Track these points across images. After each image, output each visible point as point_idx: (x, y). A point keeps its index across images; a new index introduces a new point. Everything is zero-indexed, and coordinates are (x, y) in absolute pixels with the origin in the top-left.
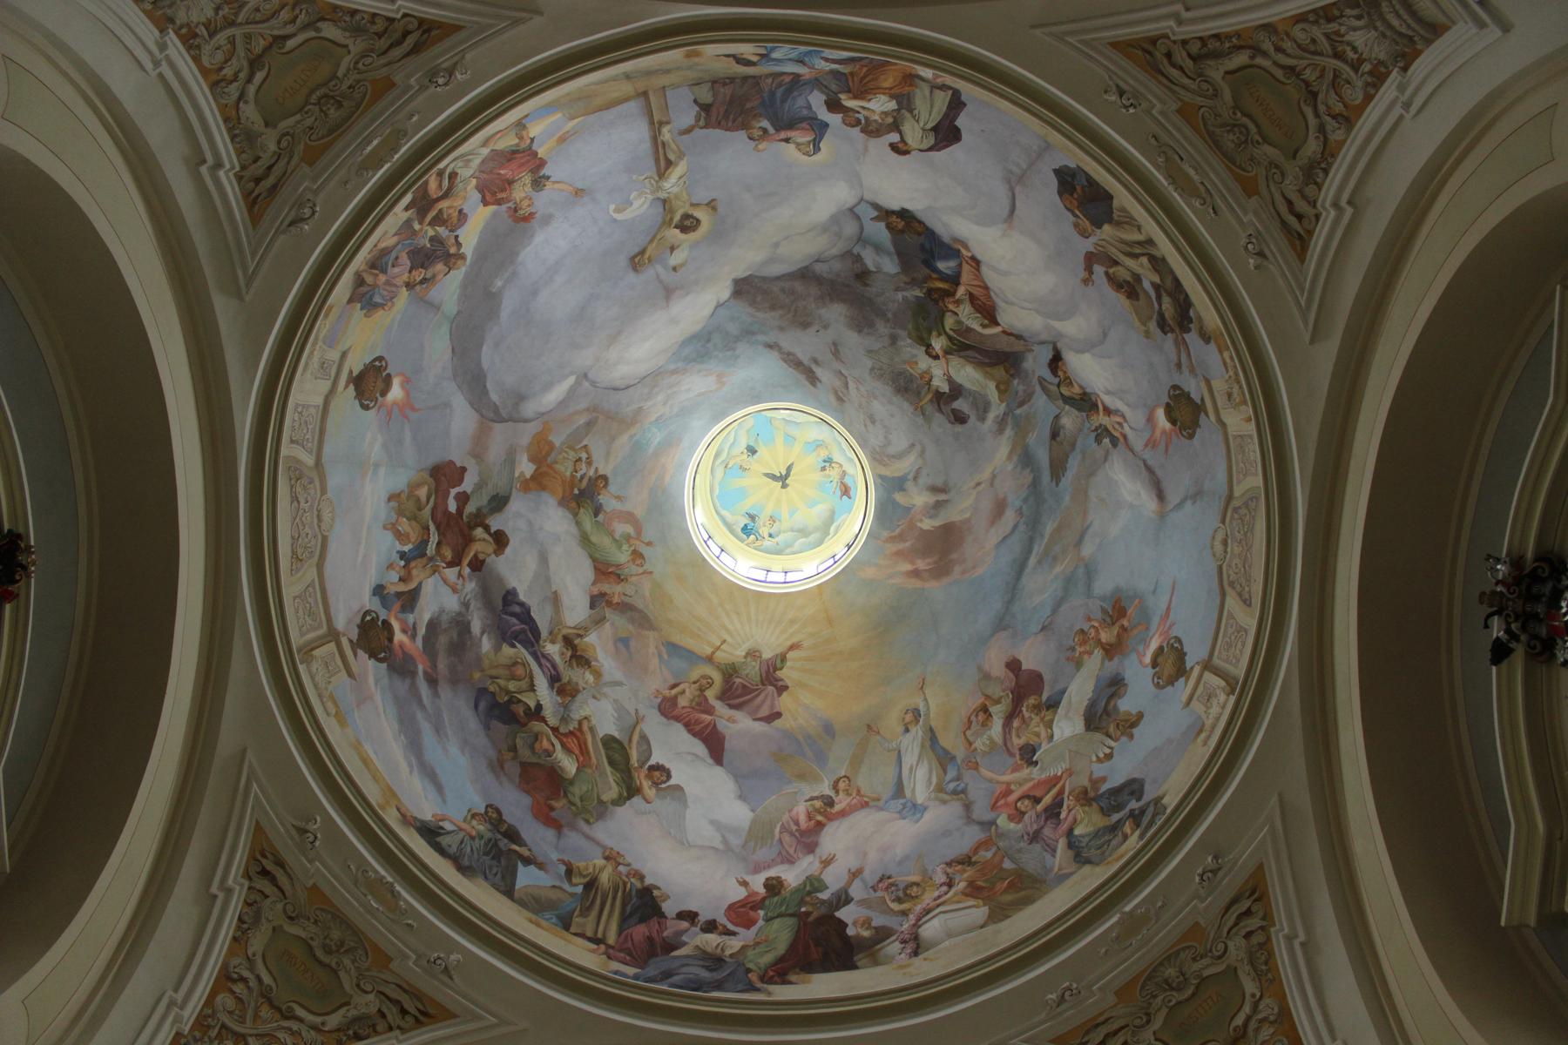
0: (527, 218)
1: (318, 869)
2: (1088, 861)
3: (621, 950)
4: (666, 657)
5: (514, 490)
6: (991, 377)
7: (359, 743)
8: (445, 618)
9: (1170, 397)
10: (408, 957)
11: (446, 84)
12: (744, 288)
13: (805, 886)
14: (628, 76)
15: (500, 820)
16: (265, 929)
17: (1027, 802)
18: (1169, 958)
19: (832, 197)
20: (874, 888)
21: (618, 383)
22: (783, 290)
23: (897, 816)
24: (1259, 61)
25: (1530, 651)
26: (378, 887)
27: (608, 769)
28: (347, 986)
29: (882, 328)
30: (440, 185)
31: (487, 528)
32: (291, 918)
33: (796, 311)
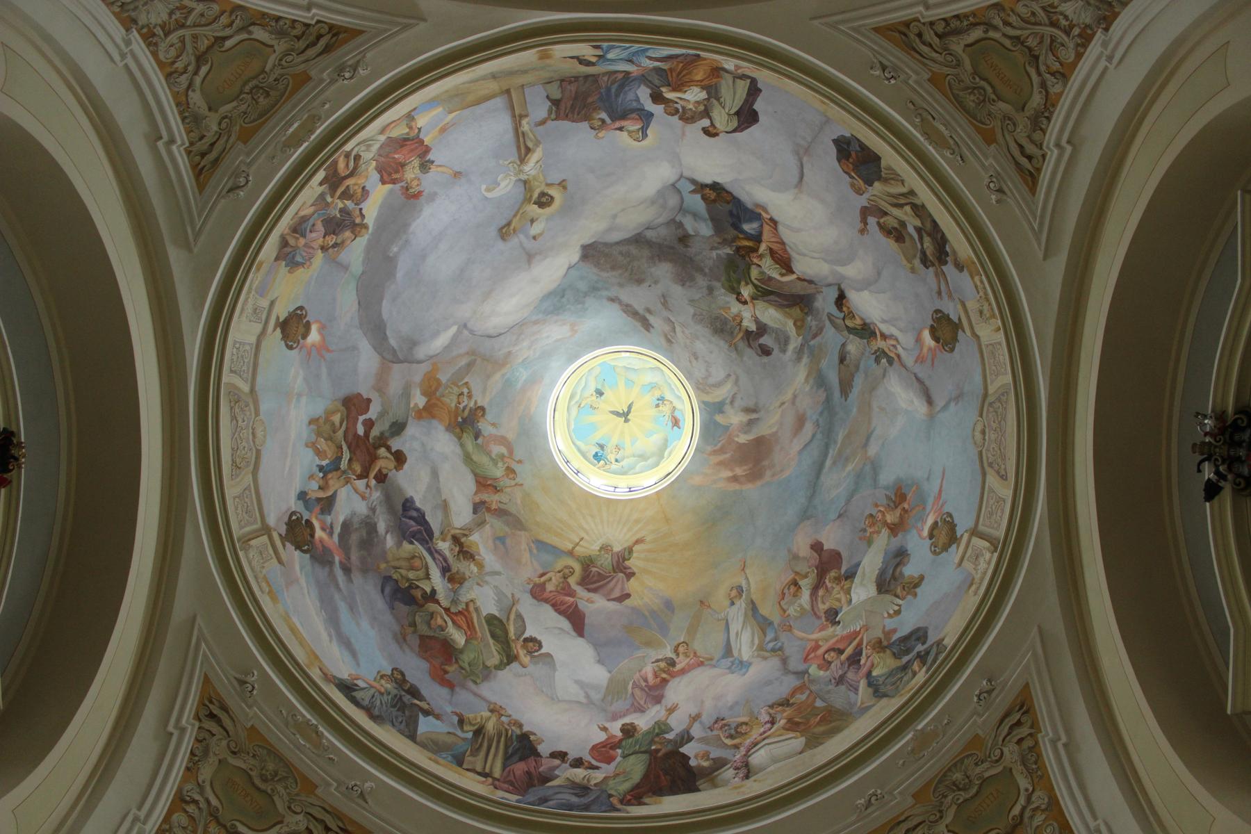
0: (417, 196)
1: (256, 713)
2: (885, 695)
3: (504, 782)
4: (535, 551)
5: (410, 418)
6: (790, 316)
7: (289, 616)
8: (356, 520)
9: (933, 320)
10: (329, 785)
11: (351, 78)
12: (591, 253)
13: (654, 729)
14: (494, 76)
15: (404, 680)
17: (832, 654)
18: (956, 765)
19: (658, 175)
20: (711, 729)
21: (491, 332)
22: (621, 253)
23: (728, 671)
24: (992, 34)
25: (1235, 486)
26: (304, 729)
27: (491, 641)
28: (280, 806)
29: (702, 281)
30: (347, 165)
31: (388, 448)
32: (234, 753)
33: (632, 270)
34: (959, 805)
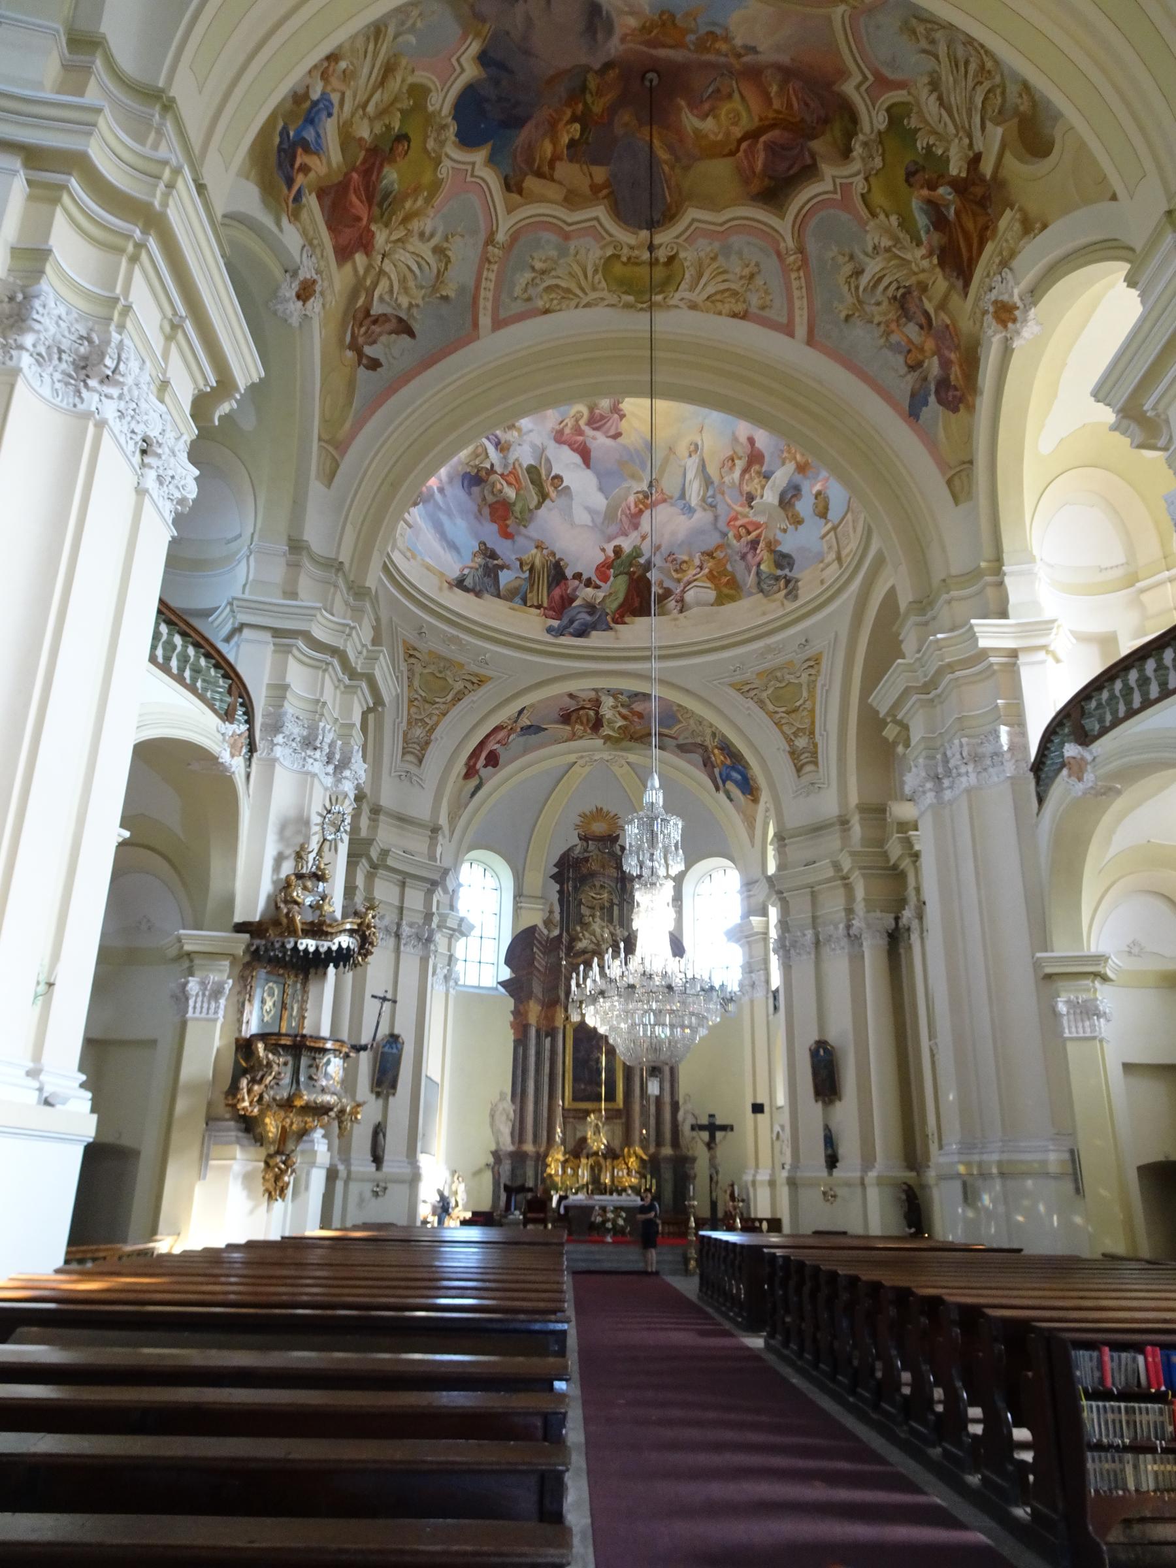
2: (762, 591)
15: (487, 548)
16: (417, 676)
18: (780, 669)
27: (531, 486)
28: (450, 681)
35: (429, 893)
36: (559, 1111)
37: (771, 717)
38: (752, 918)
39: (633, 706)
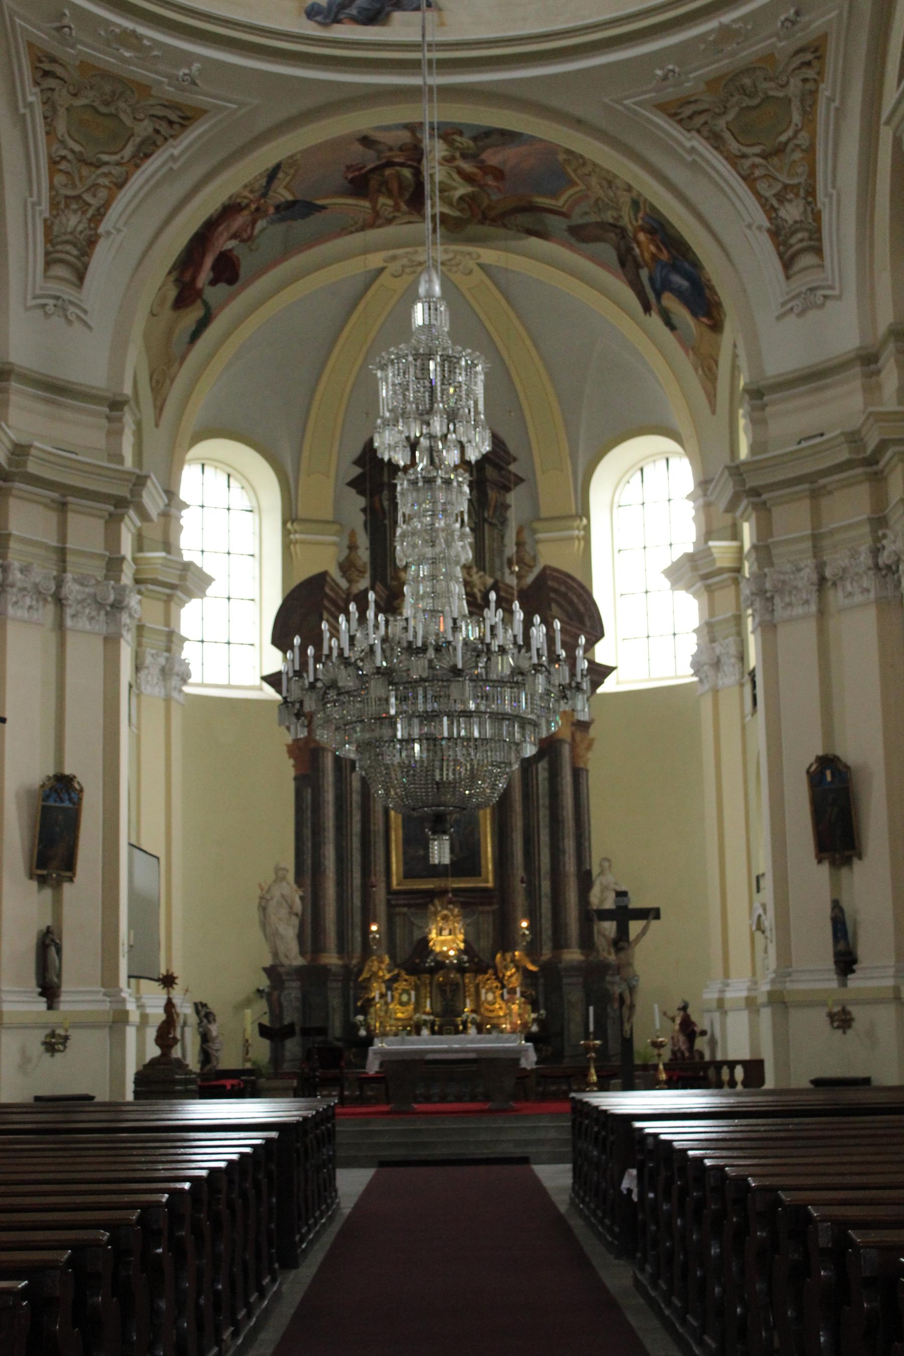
10: (161, 83)
16: (62, 112)
18: (749, 70)
28: (128, 121)
32: (75, 95)
34: (742, 109)
35: (113, 521)
36: (380, 894)
37: (734, 166)
38: (711, 543)
39: (484, 156)
